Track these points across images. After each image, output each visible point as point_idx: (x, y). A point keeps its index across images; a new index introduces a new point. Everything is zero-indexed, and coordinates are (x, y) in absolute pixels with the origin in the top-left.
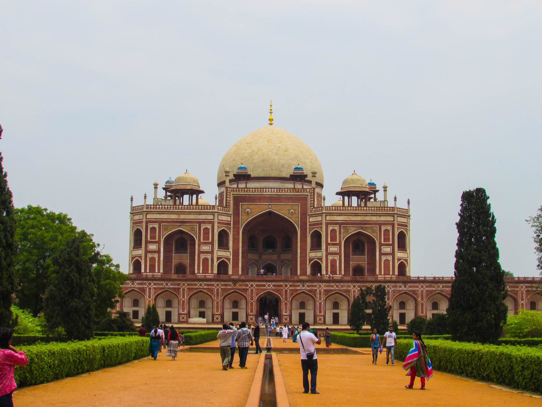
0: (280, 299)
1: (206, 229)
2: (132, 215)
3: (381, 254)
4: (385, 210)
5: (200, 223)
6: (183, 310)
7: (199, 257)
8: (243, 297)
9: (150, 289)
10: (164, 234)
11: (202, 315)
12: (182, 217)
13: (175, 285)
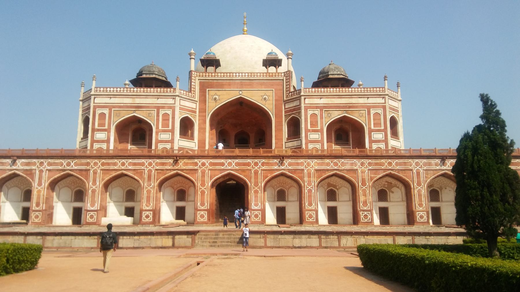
0: (247, 185)
1: (166, 115)
2: (81, 103)
3: (371, 142)
4: (373, 91)
5: (158, 108)
6: (93, 205)
7: (156, 146)
8: (192, 185)
9: (41, 171)
10: (115, 120)
11: (129, 212)
12: (138, 101)
13: (82, 164)
